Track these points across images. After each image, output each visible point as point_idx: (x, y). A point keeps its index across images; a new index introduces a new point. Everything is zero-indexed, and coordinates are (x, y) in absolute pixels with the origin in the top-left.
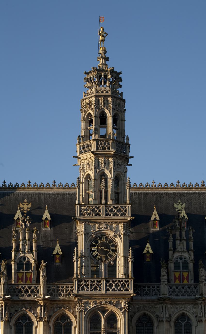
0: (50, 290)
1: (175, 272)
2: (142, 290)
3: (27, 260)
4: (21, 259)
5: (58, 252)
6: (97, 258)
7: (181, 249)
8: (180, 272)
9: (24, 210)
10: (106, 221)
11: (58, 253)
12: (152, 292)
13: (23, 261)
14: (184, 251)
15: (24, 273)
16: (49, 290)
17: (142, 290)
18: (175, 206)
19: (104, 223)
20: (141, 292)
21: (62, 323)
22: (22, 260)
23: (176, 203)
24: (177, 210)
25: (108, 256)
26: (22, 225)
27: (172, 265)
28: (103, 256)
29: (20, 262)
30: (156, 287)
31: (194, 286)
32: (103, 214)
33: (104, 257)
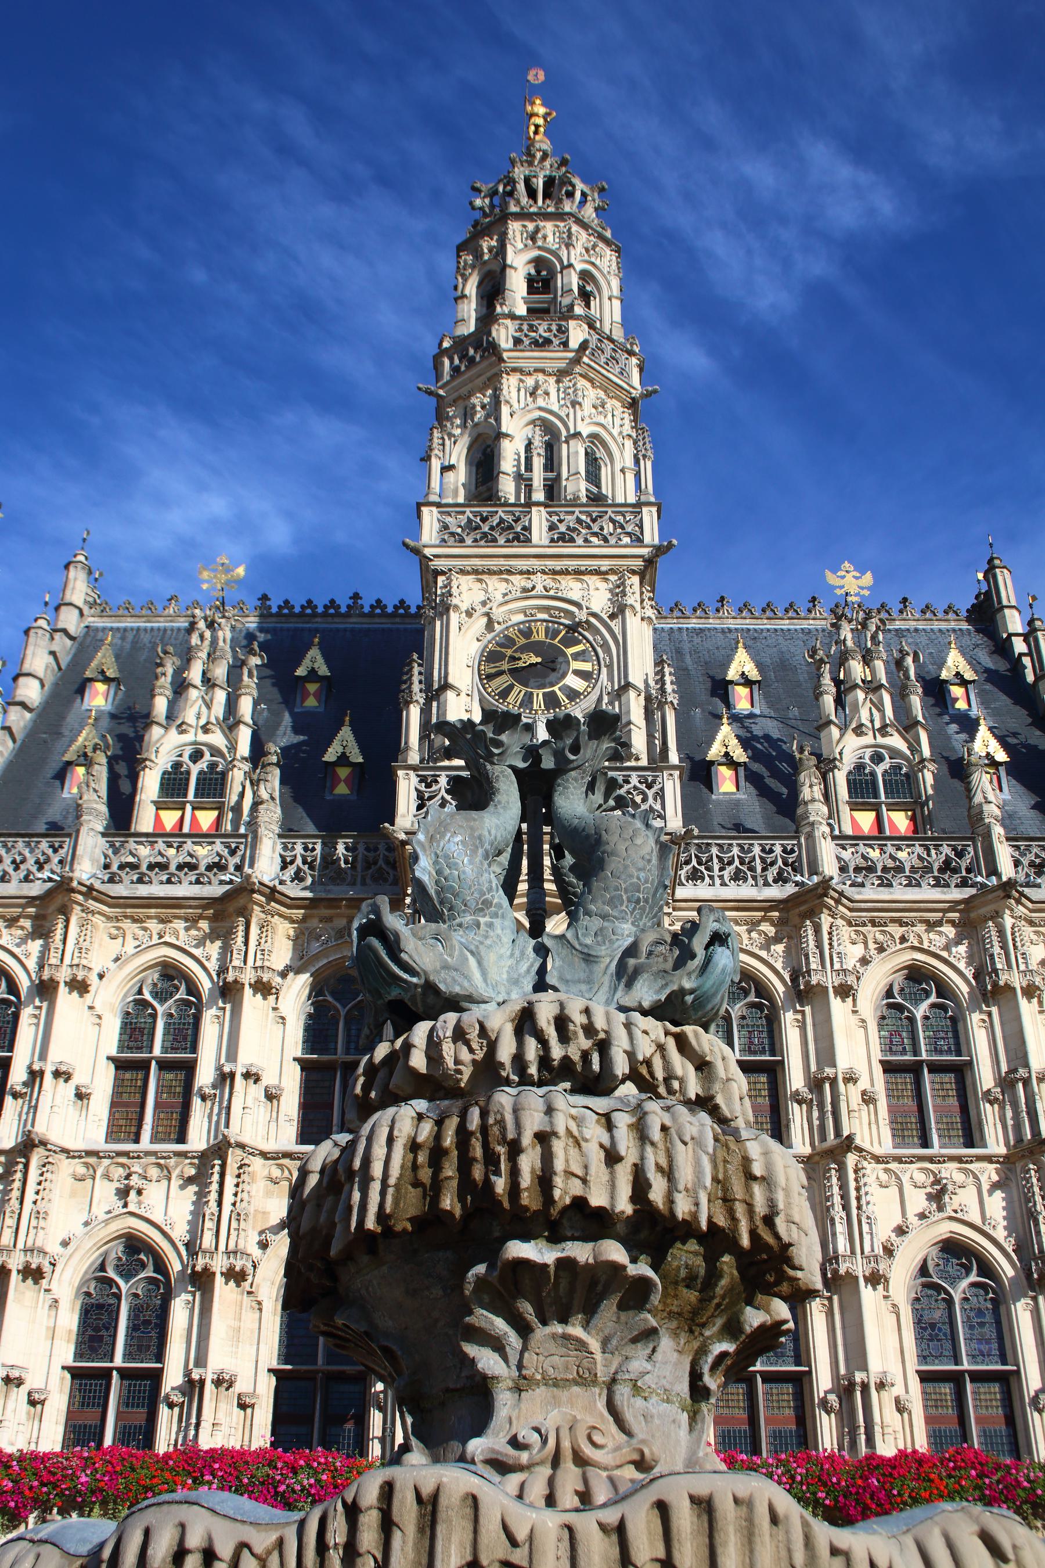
0: (292, 862)
1: (854, 807)
2: (715, 860)
3: (207, 756)
4: (180, 756)
5: (344, 754)
6: (511, 699)
7: (872, 721)
8: (876, 808)
9: (214, 589)
10: (551, 564)
11: (343, 759)
12: (764, 869)
13: (191, 764)
14: (884, 726)
15: (189, 808)
16: (288, 859)
17: (715, 860)
18: (831, 579)
19: (543, 572)
20: (708, 869)
21: (338, 1005)
22: (186, 758)
23: (834, 572)
24: (839, 592)
25: (559, 693)
26: (202, 637)
27: (840, 778)
28: (535, 692)
29: (177, 765)
30: (778, 849)
31: (955, 849)
32: (539, 533)
33: (541, 696)
